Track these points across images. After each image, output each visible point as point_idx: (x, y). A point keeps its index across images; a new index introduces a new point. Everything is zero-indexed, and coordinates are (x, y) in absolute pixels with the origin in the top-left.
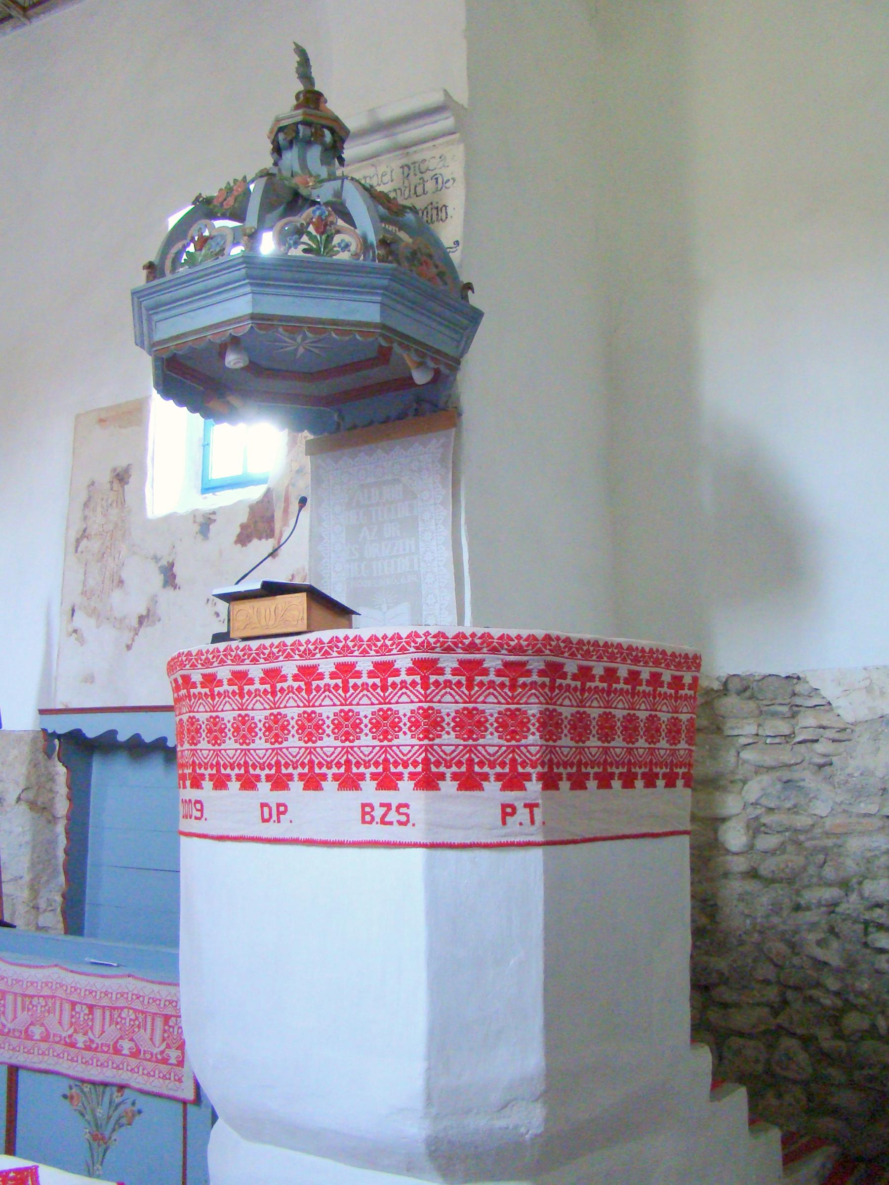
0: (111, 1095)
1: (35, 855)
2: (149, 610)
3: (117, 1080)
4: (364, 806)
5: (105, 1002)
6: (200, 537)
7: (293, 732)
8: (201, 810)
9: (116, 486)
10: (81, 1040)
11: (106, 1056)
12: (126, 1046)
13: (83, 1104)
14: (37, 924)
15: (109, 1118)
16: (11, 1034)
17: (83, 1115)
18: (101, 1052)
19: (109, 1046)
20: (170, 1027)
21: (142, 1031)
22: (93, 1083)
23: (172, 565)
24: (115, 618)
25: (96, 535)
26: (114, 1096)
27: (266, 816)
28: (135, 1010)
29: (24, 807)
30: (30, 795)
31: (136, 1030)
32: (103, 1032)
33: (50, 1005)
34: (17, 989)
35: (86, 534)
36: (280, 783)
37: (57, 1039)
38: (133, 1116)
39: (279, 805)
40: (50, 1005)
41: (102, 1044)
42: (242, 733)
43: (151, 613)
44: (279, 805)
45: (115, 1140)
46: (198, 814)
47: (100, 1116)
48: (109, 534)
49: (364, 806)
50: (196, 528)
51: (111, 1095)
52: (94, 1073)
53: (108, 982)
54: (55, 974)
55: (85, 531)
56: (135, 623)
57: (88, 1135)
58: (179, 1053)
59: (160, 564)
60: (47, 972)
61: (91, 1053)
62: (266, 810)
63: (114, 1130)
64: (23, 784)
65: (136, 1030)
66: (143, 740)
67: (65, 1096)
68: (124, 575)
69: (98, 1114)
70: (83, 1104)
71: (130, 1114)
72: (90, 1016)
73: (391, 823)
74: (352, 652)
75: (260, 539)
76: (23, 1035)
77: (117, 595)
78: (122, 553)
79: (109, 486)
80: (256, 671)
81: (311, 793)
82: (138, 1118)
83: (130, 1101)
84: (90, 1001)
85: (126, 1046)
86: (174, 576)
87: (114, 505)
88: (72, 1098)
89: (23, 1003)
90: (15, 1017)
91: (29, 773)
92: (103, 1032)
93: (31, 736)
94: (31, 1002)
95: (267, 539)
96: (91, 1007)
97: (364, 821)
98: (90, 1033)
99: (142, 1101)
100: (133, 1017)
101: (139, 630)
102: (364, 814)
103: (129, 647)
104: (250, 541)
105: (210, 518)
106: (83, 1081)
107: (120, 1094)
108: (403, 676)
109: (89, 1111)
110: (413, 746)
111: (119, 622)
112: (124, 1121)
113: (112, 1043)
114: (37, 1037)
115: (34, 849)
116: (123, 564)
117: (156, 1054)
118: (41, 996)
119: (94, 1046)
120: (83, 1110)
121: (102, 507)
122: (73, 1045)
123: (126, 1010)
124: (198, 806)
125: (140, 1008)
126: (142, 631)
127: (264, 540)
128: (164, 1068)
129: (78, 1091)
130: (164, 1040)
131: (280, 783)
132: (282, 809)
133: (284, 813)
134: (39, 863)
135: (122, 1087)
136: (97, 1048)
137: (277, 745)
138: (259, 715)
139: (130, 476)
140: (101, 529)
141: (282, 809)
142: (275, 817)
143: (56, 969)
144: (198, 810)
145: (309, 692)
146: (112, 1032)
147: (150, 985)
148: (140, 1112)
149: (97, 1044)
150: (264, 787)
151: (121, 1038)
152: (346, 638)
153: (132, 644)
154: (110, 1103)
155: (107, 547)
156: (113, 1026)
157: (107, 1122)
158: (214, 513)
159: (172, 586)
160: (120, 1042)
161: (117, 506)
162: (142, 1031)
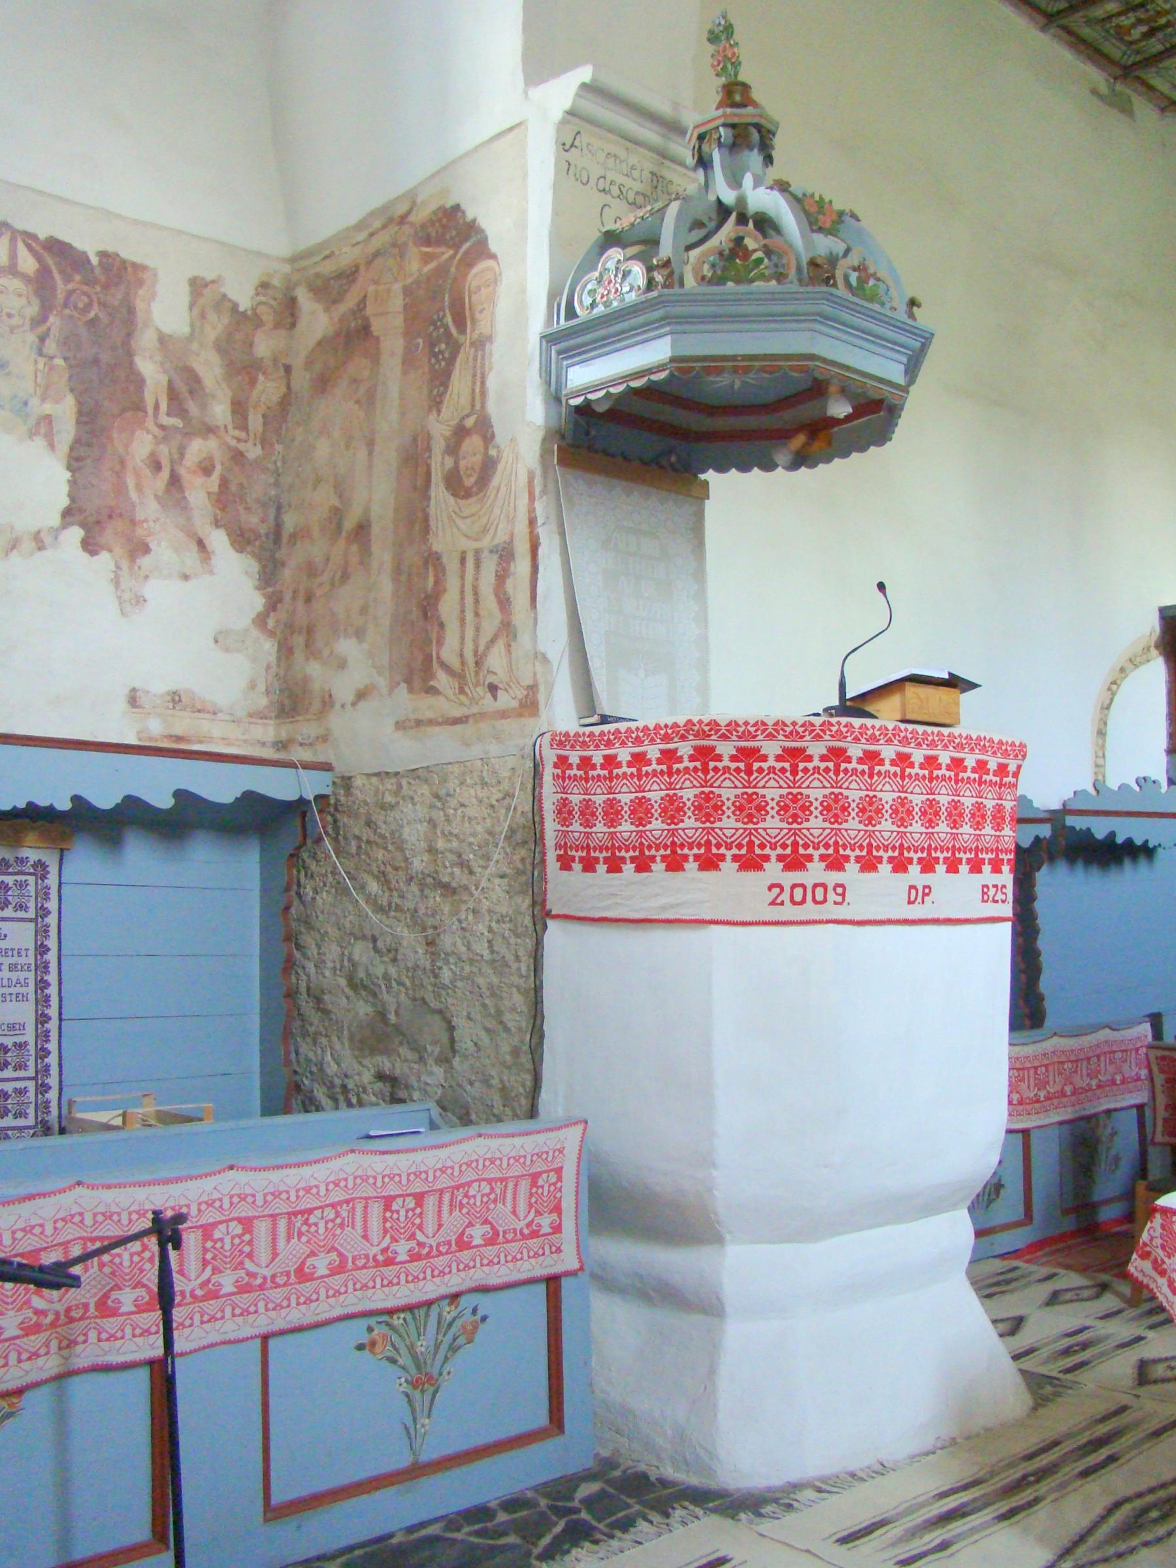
0: (440, 1315)
3: (444, 1290)
4: (983, 886)
5: (444, 1182)
7: (853, 814)
8: (843, 895)
10: (402, 1249)
12: (478, 1233)
13: (393, 1345)
15: (437, 1347)
16: (269, 1284)
17: (393, 1361)
18: (437, 1256)
20: (215, 1242)
21: (500, 1205)
22: (410, 1308)
26: (445, 1314)
27: (912, 898)
28: (489, 1181)
31: (492, 1206)
32: (440, 1226)
33: (345, 1214)
34: (280, 1207)
36: (928, 866)
37: (361, 1262)
38: (476, 1328)
39: (925, 887)
40: (345, 1214)
41: (438, 1245)
42: (900, 815)
44: (925, 887)
45: (449, 1373)
46: (839, 899)
47: (423, 1349)
49: (983, 886)
51: (440, 1315)
52: (404, 1294)
53: (443, 1153)
54: (350, 1164)
57: (405, 1385)
58: (554, 1216)
60: (335, 1164)
61: (422, 1263)
62: (913, 892)
63: (446, 1359)
65: (492, 1206)
67: (360, 1347)
69: (419, 1350)
70: (393, 1345)
71: (469, 1327)
72: (418, 1211)
73: (997, 902)
74: (846, 737)
76: (293, 1279)
80: (918, 756)
81: (951, 875)
82: (482, 1327)
83: (468, 1312)
84: (418, 1187)
85: (478, 1233)
88: (373, 1344)
89: (290, 1224)
90: (275, 1255)
92: (440, 1226)
94: (306, 1222)
96: (419, 1198)
97: (983, 901)
98: (420, 1237)
99: (485, 1303)
100: (487, 1190)
102: (984, 893)
106: (391, 1312)
107: (453, 1307)
108: (816, 762)
109: (404, 1351)
110: (737, 829)
112: (461, 1340)
113: (453, 1239)
114: (322, 1271)
117: (521, 1230)
118: (484, 1180)
119: (425, 1251)
120: (393, 1354)
122: (389, 1262)
123: (476, 1185)
124: (840, 890)
125: (499, 1175)
128: (534, 1243)
129: (384, 1329)
130: (531, 1206)
131: (928, 866)
132: (927, 891)
133: (928, 895)
135: (454, 1297)
136: (57, 1318)
137: (870, 828)
138: (917, 800)
141: (927, 891)
142: (919, 899)
143: (351, 1156)
144: (838, 894)
145: (837, 773)
146: (454, 1222)
147: (508, 1141)
148: (484, 1319)
149: (431, 1247)
150: (914, 869)
151: (470, 1224)
152: (873, 727)
154: (439, 1322)
156: (456, 1213)
157: (435, 1355)
160: (468, 1231)
162: (500, 1205)
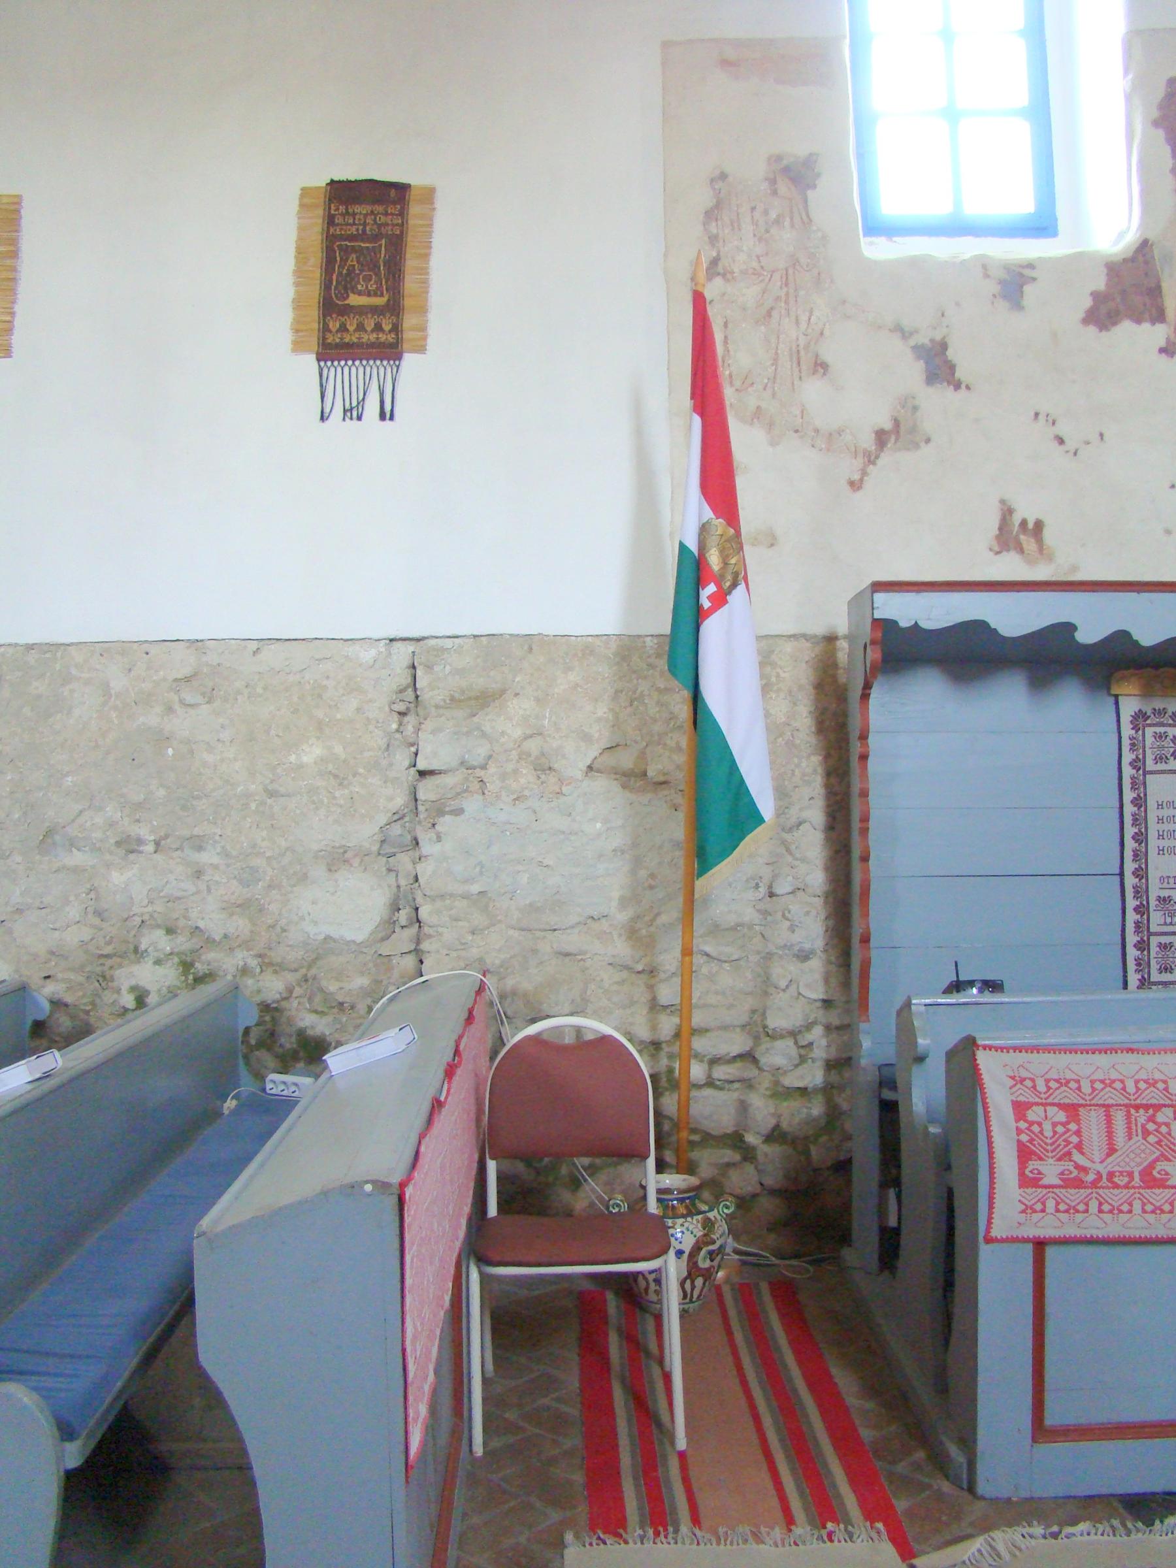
1: (643, 873)
2: (897, 423)
6: (1002, 305)
9: (783, 187)
11: (1125, 1194)
14: (654, 999)
19: (1130, 1174)
23: (944, 346)
24: (817, 431)
25: (744, 272)
29: (601, 784)
30: (626, 760)
35: (720, 269)
43: (902, 429)
48: (777, 276)
50: (994, 288)
55: (715, 262)
56: (867, 441)
59: (912, 342)
64: (601, 735)
66: (1136, 643)
68: (827, 356)
75: (1138, 321)
77: (813, 391)
78: (816, 313)
79: (765, 186)
86: (952, 368)
87: (787, 223)
91: (617, 717)
93: (613, 646)
95: (1153, 323)
101: (877, 457)
103: (855, 485)
104: (1115, 324)
105: (1021, 275)
111: (830, 440)
115: (637, 862)
116: (822, 334)
121: (755, 223)
126: (885, 459)
127: (1146, 326)
134: (651, 887)
139: (818, 175)
140: (755, 264)
153: (861, 480)
155: (778, 299)
158: (1031, 266)
159: (949, 383)
161: (792, 226)
